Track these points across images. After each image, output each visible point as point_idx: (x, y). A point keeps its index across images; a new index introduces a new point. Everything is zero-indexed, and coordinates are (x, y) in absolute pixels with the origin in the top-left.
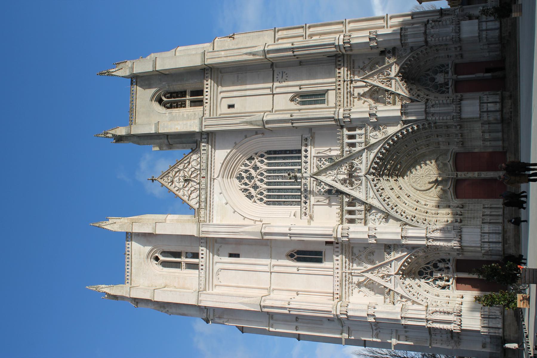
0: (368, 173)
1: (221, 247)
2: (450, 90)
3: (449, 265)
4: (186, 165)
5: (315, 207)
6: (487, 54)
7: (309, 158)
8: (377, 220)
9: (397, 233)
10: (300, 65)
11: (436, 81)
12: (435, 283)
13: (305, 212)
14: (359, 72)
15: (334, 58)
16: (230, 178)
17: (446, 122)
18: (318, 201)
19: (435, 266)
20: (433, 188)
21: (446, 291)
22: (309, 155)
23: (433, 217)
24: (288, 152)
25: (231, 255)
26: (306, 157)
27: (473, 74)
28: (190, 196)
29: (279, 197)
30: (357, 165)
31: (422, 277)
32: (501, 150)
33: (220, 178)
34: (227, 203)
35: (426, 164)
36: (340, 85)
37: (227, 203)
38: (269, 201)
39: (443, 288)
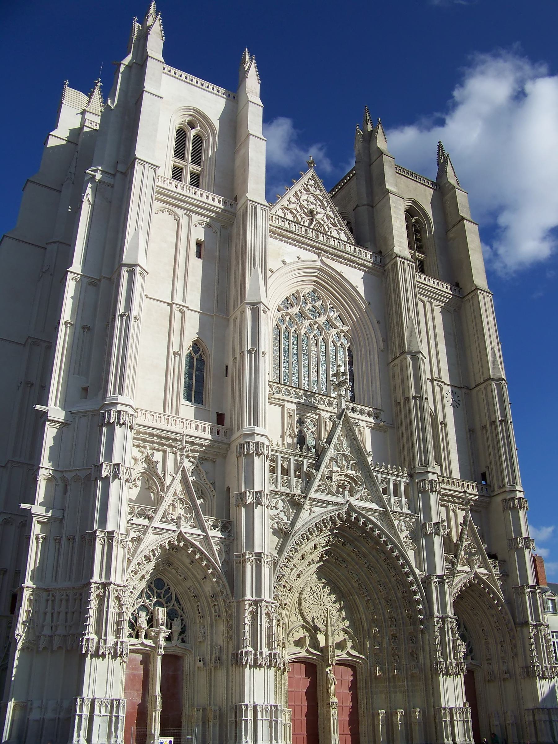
0: (351, 508)
1: (215, 232)
4: (332, 220)
5: (280, 408)
9: (263, 546)
10: (470, 431)
12: (140, 609)
16: (315, 281)
18: (290, 416)
20: (302, 622)
25: (199, 244)
28: (288, 209)
31: (153, 586)
33: (319, 263)
34: (284, 263)
35: (340, 610)
37: (284, 263)
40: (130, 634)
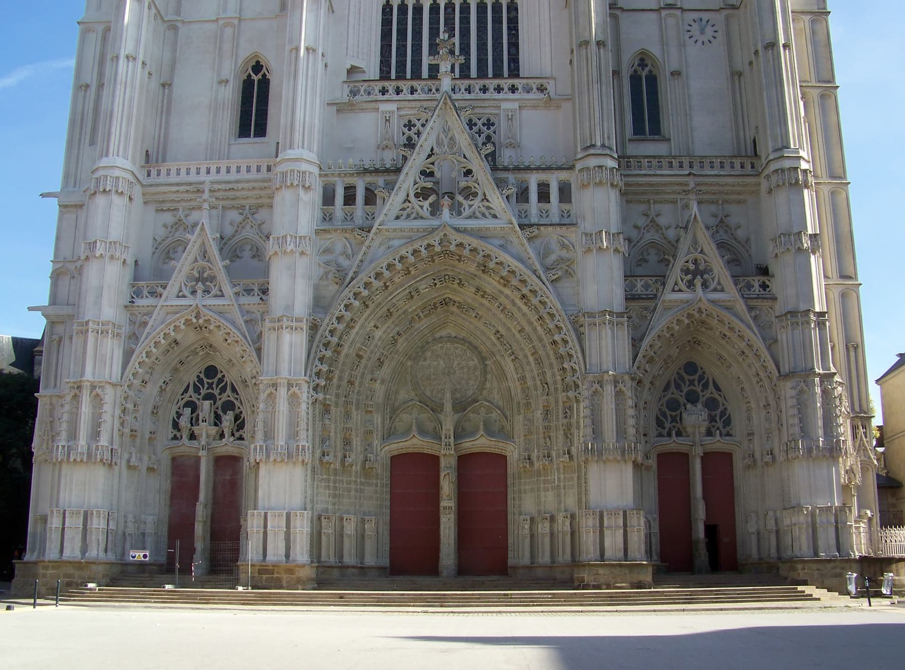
2: (665, 440)
3: (228, 439)
6: (752, 528)
7: (496, 96)
8: (329, 257)
10: (732, 74)
11: (689, 406)
12: (188, 404)
13: (359, 91)
14: (715, 216)
15: (750, 152)
17: (578, 428)
19: (229, 406)
21: (170, 432)
22: (501, 96)
23: (337, 396)
24: (513, 51)
26: (499, 89)
27: (705, 497)
29: (402, 33)
30: (470, 206)
31: (202, 376)
32: (510, 562)
36: (681, 167)
38: (392, 10)
39: (176, 425)
40: (175, 435)
